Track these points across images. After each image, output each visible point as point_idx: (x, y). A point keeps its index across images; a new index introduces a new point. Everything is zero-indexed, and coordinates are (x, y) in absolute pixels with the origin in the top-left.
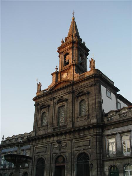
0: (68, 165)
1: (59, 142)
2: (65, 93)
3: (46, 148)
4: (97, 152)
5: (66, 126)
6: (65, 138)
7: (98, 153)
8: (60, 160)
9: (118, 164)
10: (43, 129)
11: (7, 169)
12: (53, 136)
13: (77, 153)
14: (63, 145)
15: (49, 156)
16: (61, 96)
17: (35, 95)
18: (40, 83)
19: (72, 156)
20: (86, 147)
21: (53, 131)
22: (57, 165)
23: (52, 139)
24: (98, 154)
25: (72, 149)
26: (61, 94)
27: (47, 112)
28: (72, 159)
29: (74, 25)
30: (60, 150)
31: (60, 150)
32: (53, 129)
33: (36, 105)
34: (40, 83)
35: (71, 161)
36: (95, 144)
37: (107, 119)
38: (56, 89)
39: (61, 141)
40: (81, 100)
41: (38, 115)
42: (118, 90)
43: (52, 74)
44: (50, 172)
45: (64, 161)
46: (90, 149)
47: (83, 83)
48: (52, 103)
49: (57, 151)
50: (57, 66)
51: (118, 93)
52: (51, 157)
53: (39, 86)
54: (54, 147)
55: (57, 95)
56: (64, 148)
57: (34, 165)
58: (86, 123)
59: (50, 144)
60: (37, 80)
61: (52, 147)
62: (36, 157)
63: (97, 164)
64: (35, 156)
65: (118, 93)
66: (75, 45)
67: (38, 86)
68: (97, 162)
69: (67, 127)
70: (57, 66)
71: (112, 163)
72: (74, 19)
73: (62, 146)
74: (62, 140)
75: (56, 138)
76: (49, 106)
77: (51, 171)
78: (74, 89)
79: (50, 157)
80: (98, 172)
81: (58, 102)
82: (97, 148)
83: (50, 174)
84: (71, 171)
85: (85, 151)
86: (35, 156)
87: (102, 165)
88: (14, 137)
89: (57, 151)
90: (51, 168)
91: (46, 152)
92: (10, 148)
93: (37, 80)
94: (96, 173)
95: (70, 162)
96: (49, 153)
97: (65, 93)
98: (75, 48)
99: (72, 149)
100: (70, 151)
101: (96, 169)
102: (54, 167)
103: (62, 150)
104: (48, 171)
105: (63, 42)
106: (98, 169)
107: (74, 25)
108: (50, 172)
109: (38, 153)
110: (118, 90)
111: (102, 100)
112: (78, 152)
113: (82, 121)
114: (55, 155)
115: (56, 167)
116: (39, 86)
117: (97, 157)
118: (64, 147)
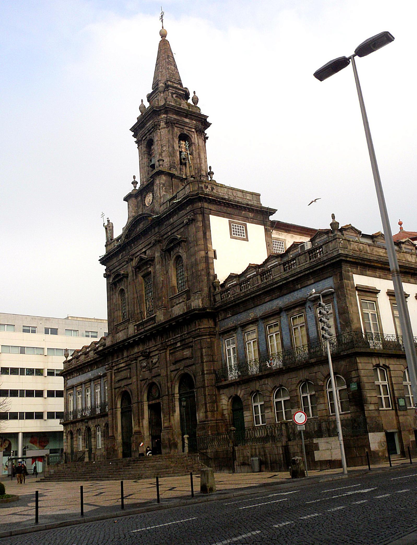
1: (147, 356)
2: (148, 245)
3: (130, 368)
4: (203, 371)
5: (153, 319)
6: (156, 346)
7: (205, 372)
9: (240, 393)
10: (121, 329)
13: (176, 375)
14: (154, 361)
16: (144, 250)
17: (103, 252)
18: (108, 221)
19: (168, 382)
20: (188, 362)
21: (136, 331)
22: (151, 403)
24: (207, 374)
25: (167, 367)
26: (143, 246)
27: (126, 290)
28: (168, 388)
29: (165, 53)
30: (150, 370)
31: (150, 370)
32: (136, 327)
33: (106, 276)
34: (108, 221)
35: (167, 393)
36: (200, 355)
37: (221, 295)
38: (133, 235)
39: (150, 353)
40: (175, 256)
41: (112, 298)
42: (272, 212)
43: (126, 199)
44: (139, 420)
46: (194, 364)
48: (130, 269)
49: (147, 374)
50: (134, 177)
51: (272, 218)
52: (137, 388)
53: (109, 228)
55: (137, 249)
56: (156, 365)
57: (115, 408)
58: (185, 307)
59: (134, 360)
60: (103, 215)
61: (138, 365)
62: (117, 390)
63: (205, 395)
64: (115, 389)
65: (272, 218)
66: (163, 116)
67: (106, 229)
68: (205, 390)
69: (157, 319)
70: (134, 177)
71: (232, 391)
72: (163, 35)
73: (152, 361)
74: (151, 350)
76: (126, 276)
77: (141, 417)
78: (162, 233)
79: (136, 388)
80: (206, 412)
81: (138, 268)
82: (202, 362)
83: (139, 423)
84: (169, 414)
85: (186, 371)
86: (115, 389)
87: (214, 397)
88: (84, 349)
89: (147, 374)
90: (140, 411)
91: (130, 378)
92: (79, 375)
93: (103, 215)
94: (204, 414)
95: (166, 395)
97: (148, 245)
98: (163, 124)
99: (167, 367)
101: (204, 407)
102: (146, 408)
104: (137, 418)
105: (142, 108)
106: (208, 405)
107: (165, 53)
108: (139, 420)
109: (119, 381)
110: (272, 212)
111: (215, 252)
112: (176, 375)
113: (179, 305)
114: (144, 382)
115: (150, 406)
116: (109, 228)
117: (204, 381)
118: (155, 363)
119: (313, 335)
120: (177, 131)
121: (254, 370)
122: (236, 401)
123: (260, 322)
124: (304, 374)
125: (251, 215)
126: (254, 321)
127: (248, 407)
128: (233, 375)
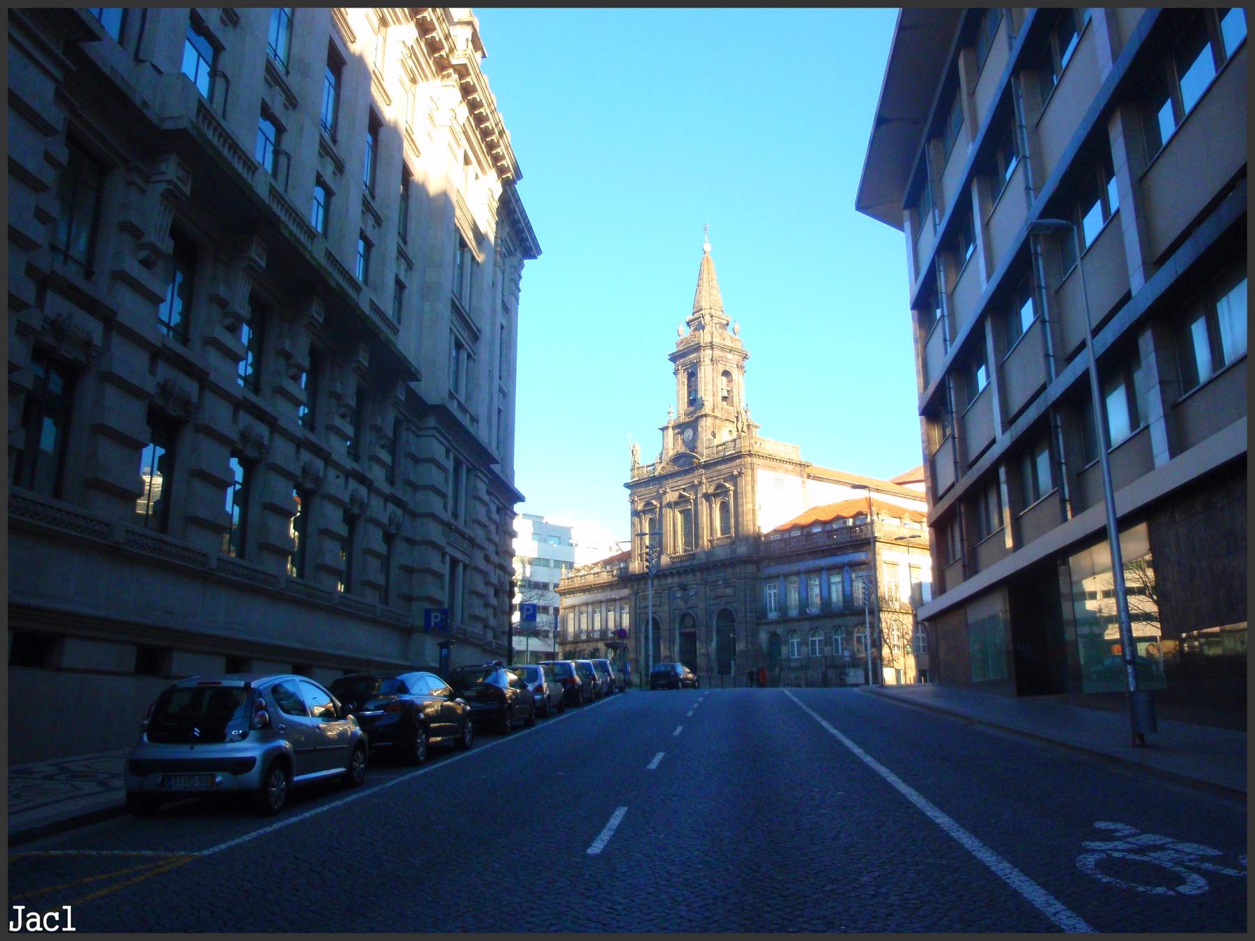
0: (701, 632)
1: (683, 588)
8: (688, 621)
9: (780, 630)
11: (583, 642)
12: (672, 574)
15: (666, 615)
23: (670, 580)
31: (686, 602)
45: (694, 626)
47: (723, 467)
49: (681, 604)
51: (808, 470)
54: (675, 598)
71: (772, 628)
75: (676, 579)
96: (666, 608)
100: (702, 605)
103: (690, 603)
115: (681, 634)
119: (848, 593)
120: (721, 368)
121: (793, 613)
122: (774, 636)
123: (803, 576)
124: (836, 621)
125: (791, 467)
126: (798, 573)
127: (786, 643)
128: (773, 615)
